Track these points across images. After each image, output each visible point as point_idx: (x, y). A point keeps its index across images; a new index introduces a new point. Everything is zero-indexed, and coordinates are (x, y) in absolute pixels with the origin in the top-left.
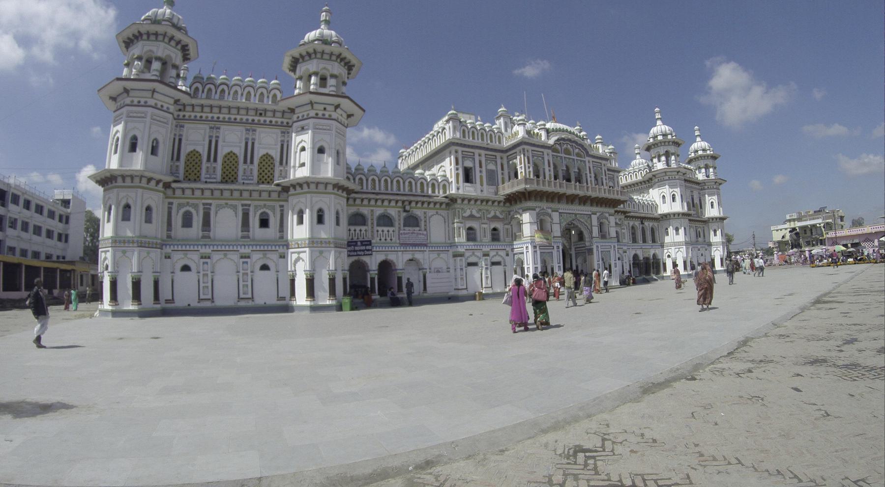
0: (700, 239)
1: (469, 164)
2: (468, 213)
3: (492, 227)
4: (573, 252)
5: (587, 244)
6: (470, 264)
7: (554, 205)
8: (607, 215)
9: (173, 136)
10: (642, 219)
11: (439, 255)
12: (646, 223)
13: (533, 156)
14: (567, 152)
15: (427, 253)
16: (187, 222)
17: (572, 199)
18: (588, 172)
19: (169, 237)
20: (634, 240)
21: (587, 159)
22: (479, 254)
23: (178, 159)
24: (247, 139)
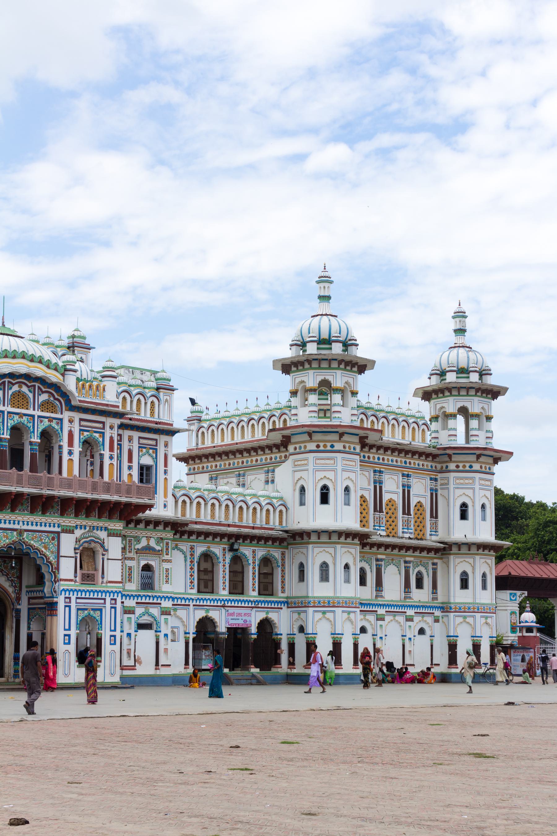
0: (420, 596)
4: (24, 607)
5: (47, 590)
8: (103, 535)
10: (234, 539)
12: (246, 551)
14: (19, 400)
18: (65, 443)
21: (66, 415)
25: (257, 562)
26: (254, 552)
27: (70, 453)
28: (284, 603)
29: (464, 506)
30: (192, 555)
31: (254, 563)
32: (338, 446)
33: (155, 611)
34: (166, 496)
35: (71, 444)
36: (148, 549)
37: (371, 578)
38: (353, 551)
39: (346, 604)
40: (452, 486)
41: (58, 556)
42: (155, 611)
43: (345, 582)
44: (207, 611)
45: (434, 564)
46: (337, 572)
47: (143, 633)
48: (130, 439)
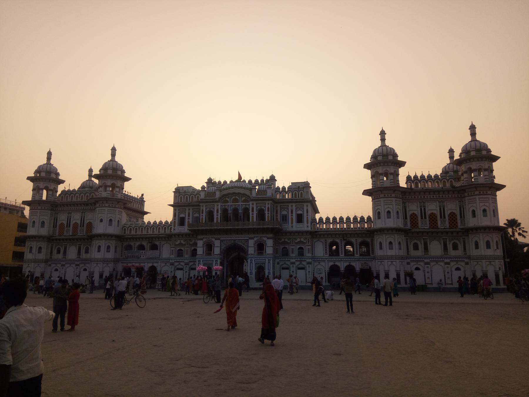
1: (182, 215)
2: (179, 242)
3: (193, 248)
6: (178, 269)
7: (216, 237)
8: (265, 239)
9: (53, 218)
11: (166, 264)
13: (206, 209)
15: (159, 263)
16: (59, 252)
17: (228, 232)
19: (51, 258)
20: (332, 253)
21: (251, 203)
22: (183, 264)
23: (56, 227)
24: (82, 217)
25: (358, 243)
26: (356, 240)
27: (253, 214)
28: (374, 258)
29: (474, 212)
30: (326, 243)
31: (357, 244)
32: (382, 196)
33: (304, 263)
34: (308, 223)
35: (253, 211)
36: (300, 242)
37: (421, 246)
38: (393, 236)
39: (391, 258)
40: (467, 203)
41: (248, 247)
42: (304, 263)
43: (390, 249)
44: (334, 262)
45: (463, 239)
46: (385, 245)
47: (299, 271)
48: (292, 206)
